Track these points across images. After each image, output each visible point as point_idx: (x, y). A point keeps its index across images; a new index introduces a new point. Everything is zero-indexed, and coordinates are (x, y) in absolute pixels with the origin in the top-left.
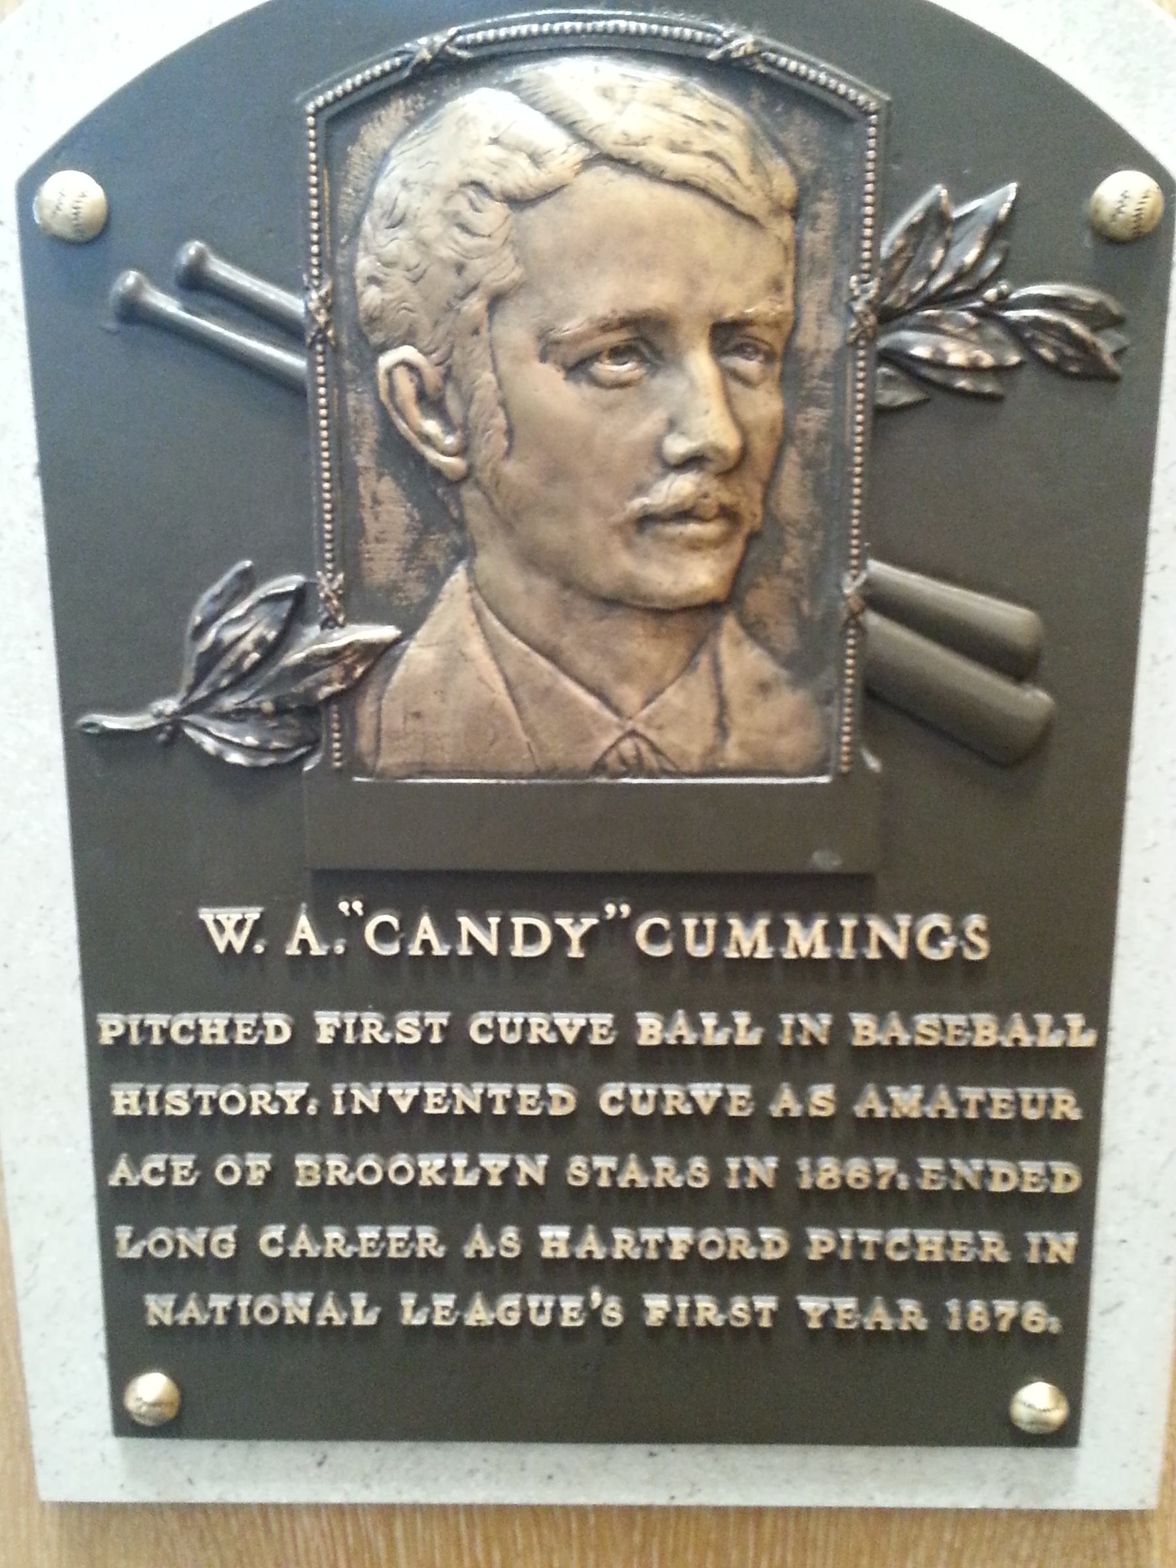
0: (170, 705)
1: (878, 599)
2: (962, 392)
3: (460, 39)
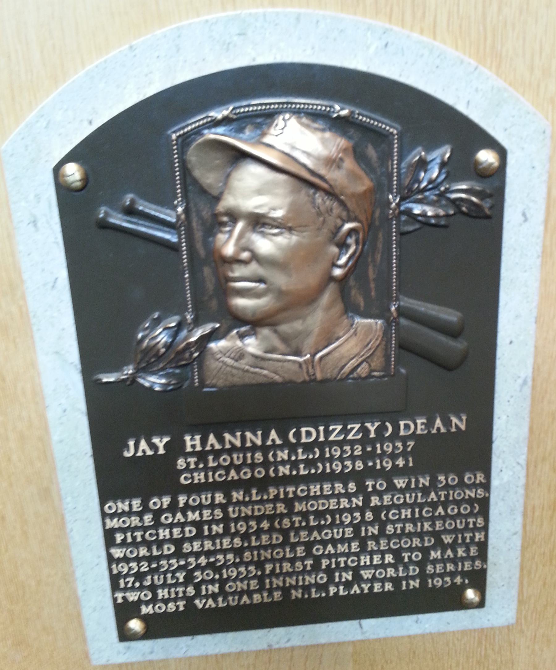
0: (129, 370)
3: (234, 112)
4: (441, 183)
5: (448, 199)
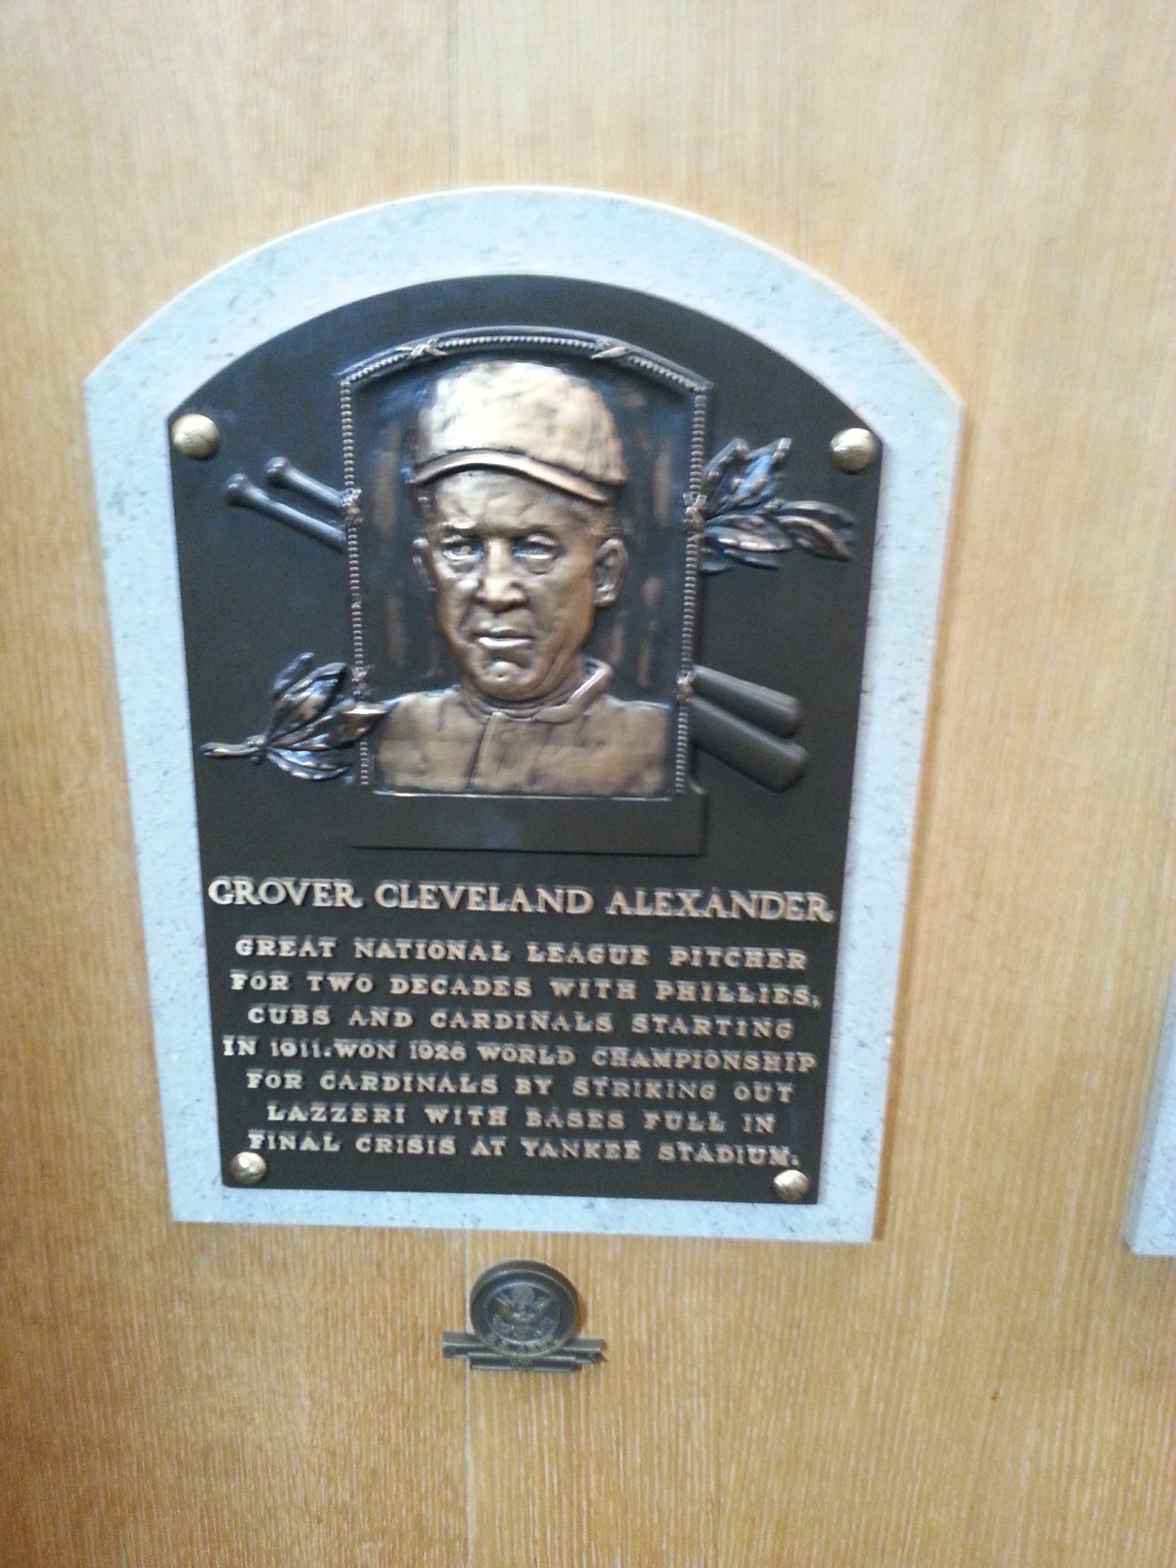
0: (260, 740)
1: (700, 688)
2: (751, 564)
4: (768, 498)
5: (777, 523)
